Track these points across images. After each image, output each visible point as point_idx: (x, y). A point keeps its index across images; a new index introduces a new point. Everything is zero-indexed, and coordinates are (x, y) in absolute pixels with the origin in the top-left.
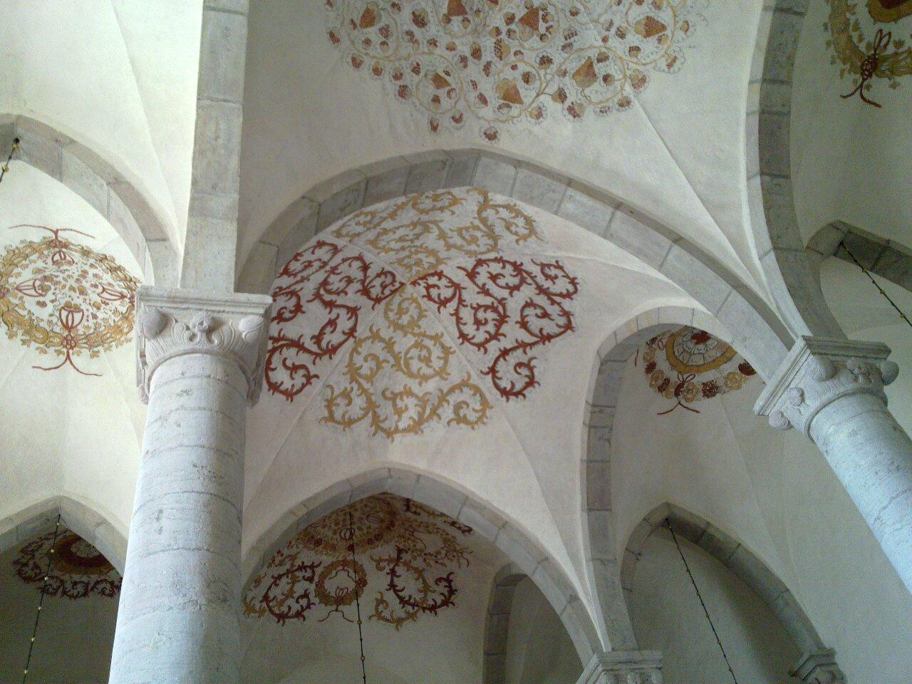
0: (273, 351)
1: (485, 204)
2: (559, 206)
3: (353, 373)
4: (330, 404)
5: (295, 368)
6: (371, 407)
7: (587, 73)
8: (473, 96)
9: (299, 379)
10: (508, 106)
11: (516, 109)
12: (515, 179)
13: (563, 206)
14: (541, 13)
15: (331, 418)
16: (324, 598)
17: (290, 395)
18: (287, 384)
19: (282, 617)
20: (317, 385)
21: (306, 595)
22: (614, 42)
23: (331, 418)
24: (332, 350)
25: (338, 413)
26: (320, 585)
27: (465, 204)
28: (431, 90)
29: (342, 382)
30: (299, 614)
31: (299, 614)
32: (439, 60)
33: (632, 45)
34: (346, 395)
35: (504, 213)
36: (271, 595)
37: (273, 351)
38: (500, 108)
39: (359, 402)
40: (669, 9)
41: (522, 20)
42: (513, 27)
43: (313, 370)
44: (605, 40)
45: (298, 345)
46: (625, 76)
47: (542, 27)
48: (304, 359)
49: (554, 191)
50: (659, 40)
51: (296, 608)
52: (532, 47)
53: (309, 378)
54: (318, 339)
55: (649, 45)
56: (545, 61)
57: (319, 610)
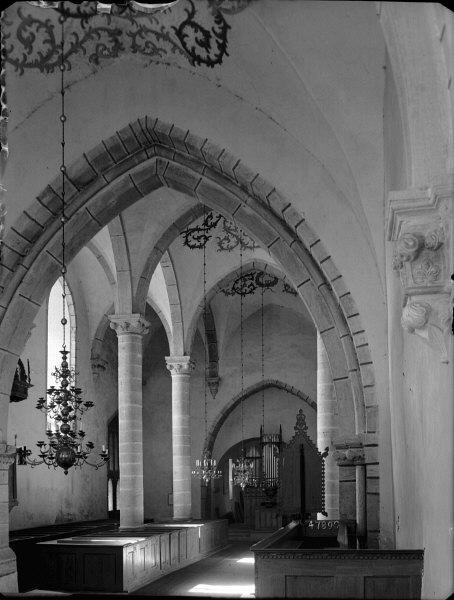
0: (187, 237)
3: (227, 230)
4: (220, 244)
5: (199, 238)
6: (240, 241)
9: (202, 241)
15: (222, 248)
16: (261, 285)
17: (200, 247)
18: (198, 244)
19: (243, 294)
20: (211, 240)
21: (252, 284)
23: (222, 248)
24: (215, 225)
25: (225, 246)
26: (257, 281)
29: (223, 235)
30: (250, 292)
31: (250, 292)
34: (227, 239)
36: (236, 286)
37: (187, 237)
39: (233, 241)
43: (207, 235)
45: (198, 229)
48: (201, 233)
51: (248, 290)
53: (207, 239)
54: (206, 223)
57: (259, 290)
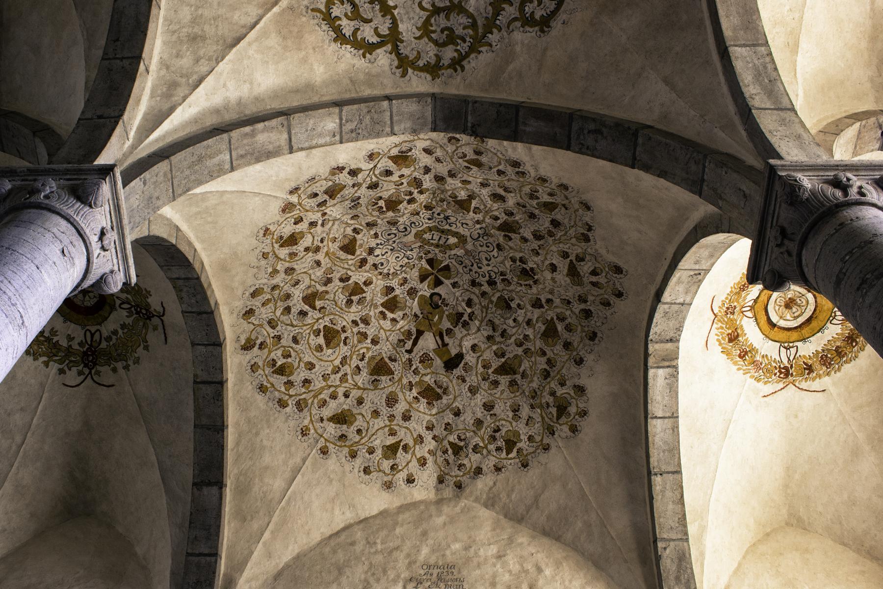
1: (393, 39)
2: (341, 119)
7: (332, 192)
8: (439, 153)
10: (402, 152)
11: (395, 152)
12: (392, 123)
13: (338, 121)
14: (384, 209)
22: (316, 216)
27: (415, 30)
28: (484, 159)
32: (476, 176)
33: (302, 223)
35: (368, 33)
38: (410, 150)
40: (282, 257)
41: (401, 202)
42: (407, 198)
44: (324, 214)
46: (300, 204)
47: (382, 203)
49: (352, 131)
50: (281, 237)
52: (388, 190)
55: (287, 229)
56: (374, 186)
